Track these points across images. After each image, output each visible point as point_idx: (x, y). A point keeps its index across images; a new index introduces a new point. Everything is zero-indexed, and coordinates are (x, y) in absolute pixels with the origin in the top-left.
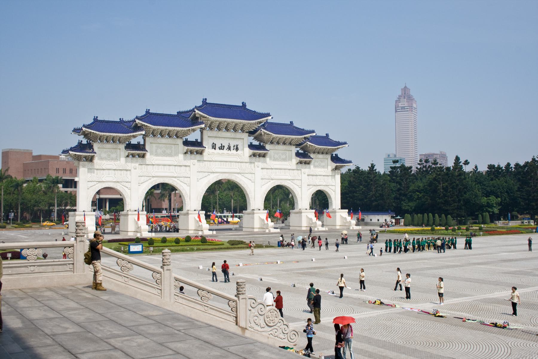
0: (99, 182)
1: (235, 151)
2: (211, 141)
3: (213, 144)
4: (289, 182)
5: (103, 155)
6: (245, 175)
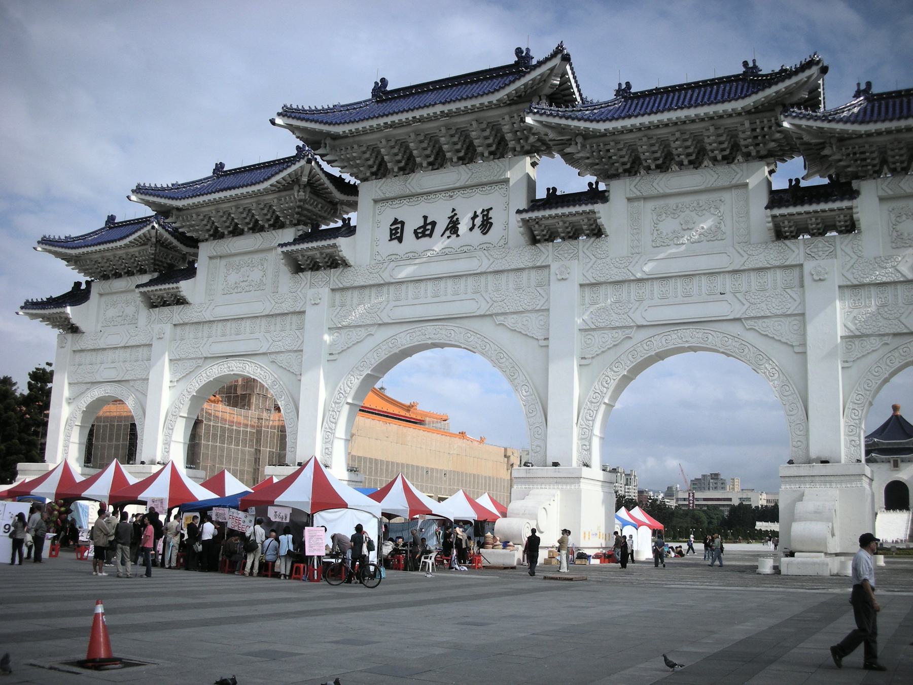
0: (93, 383)
1: (477, 231)
2: (389, 214)
3: (396, 221)
4: (736, 329)
5: (112, 312)
6: (510, 321)
